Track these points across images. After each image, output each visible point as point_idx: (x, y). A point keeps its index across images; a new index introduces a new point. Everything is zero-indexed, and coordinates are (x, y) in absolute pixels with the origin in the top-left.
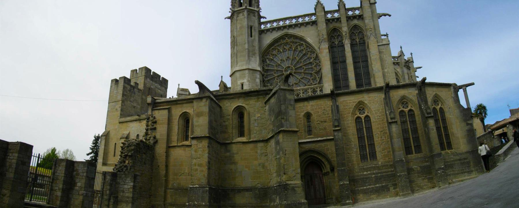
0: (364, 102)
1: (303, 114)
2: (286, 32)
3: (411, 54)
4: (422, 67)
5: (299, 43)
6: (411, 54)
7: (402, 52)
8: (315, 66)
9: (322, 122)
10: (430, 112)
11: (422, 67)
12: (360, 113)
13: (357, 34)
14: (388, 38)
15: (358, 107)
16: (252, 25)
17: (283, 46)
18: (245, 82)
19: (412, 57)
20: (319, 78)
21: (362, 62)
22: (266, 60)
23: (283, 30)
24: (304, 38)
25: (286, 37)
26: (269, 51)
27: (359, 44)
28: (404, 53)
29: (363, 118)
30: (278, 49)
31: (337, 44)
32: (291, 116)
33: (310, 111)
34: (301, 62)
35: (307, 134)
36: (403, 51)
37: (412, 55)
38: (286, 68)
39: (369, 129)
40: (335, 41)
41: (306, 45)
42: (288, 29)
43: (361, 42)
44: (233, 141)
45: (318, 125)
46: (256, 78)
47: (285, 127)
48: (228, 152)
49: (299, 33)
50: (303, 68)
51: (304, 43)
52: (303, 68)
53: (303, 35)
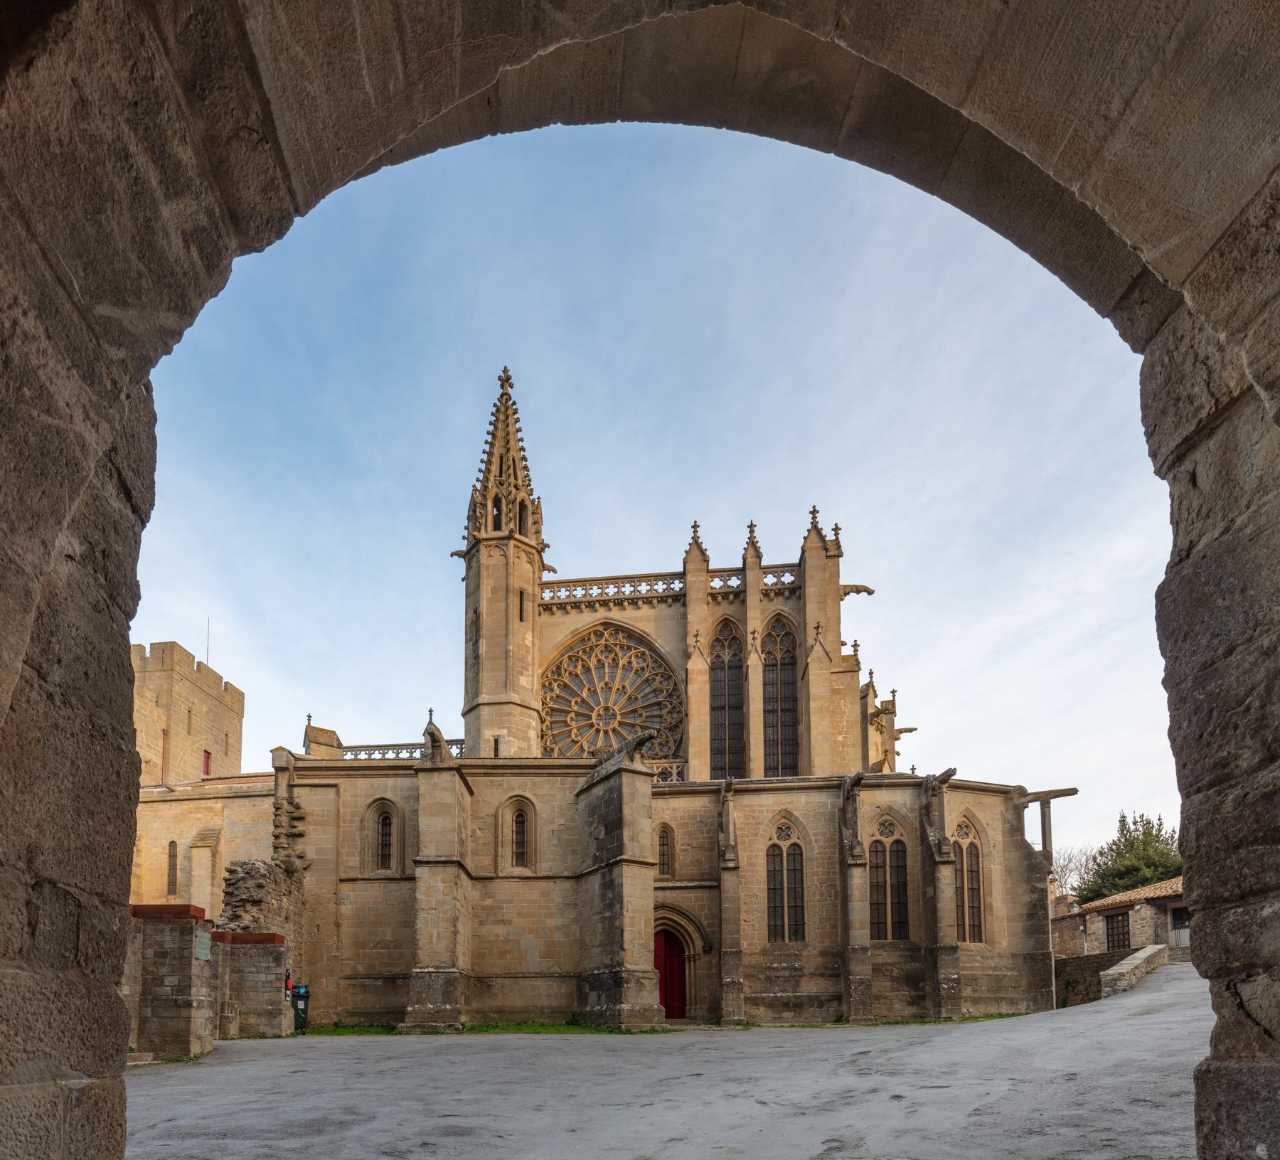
0: (792, 814)
5: (635, 649)
8: (669, 712)
12: (779, 838)
13: (779, 640)
14: (856, 655)
20: (675, 741)
21: (782, 711)
29: (785, 849)
30: (583, 660)
31: (726, 662)
34: (636, 699)
39: (797, 873)
40: (724, 654)
41: (652, 657)
43: (786, 661)
49: (636, 625)
50: (641, 715)
52: (641, 715)
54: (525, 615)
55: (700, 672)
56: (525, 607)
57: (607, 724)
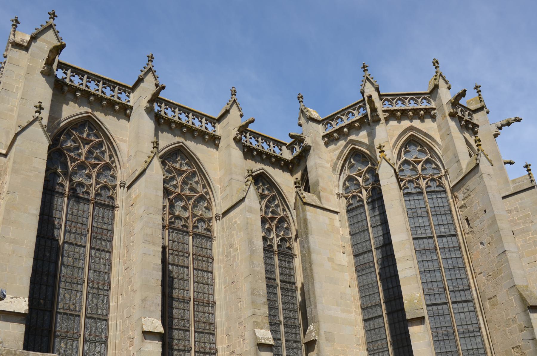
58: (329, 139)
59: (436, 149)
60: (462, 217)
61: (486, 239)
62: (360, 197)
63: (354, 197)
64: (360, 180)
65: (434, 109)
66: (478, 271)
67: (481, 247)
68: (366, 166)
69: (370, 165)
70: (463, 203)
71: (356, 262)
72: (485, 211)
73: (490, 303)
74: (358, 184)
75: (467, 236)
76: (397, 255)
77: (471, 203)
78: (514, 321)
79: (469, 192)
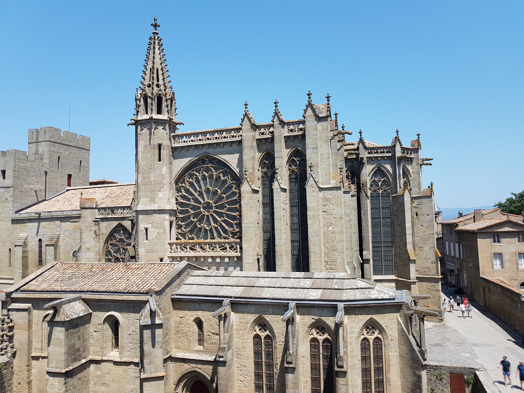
1: (193, 319)
2: (206, 153)
3: (418, 135)
4: (433, 159)
5: (222, 169)
6: (418, 135)
7: (397, 139)
9: (213, 334)
10: (341, 365)
11: (433, 159)
15: (259, 322)
16: (160, 142)
17: (202, 172)
18: (150, 228)
19: (418, 140)
22: (181, 189)
23: (202, 149)
24: (228, 164)
25: (207, 158)
26: (185, 177)
27: (300, 178)
28: (401, 141)
32: (157, 356)
33: (200, 317)
35: (197, 343)
36: (400, 138)
37: (419, 138)
38: (204, 204)
42: (208, 148)
44: (104, 359)
45: (209, 337)
46: (164, 220)
47: (148, 372)
48: (99, 371)
51: (227, 170)
53: (226, 159)
54: (162, 157)
55: (247, 192)
56: (162, 153)
57: (208, 212)
58: (370, 160)
59: (409, 176)
60: (414, 211)
61: (425, 225)
62: (378, 192)
63: (375, 191)
64: (380, 184)
65: (413, 158)
66: (416, 235)
67: (421, 227)
68: (383, 178)
69: (385, 178)
70: (416, 206)
71: (372, 221)
72: (428, 215)
73: (419, 249)
74: (378, 185)
75: (414, 219)
76: (407, 232)
77: (422, 208)
78: (430, 259)
79: (421, 203)
